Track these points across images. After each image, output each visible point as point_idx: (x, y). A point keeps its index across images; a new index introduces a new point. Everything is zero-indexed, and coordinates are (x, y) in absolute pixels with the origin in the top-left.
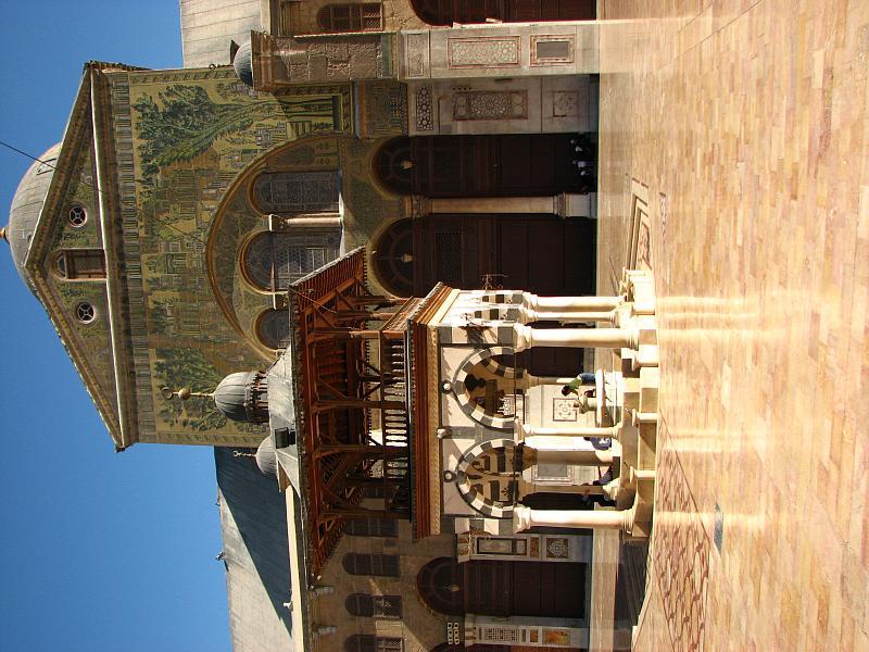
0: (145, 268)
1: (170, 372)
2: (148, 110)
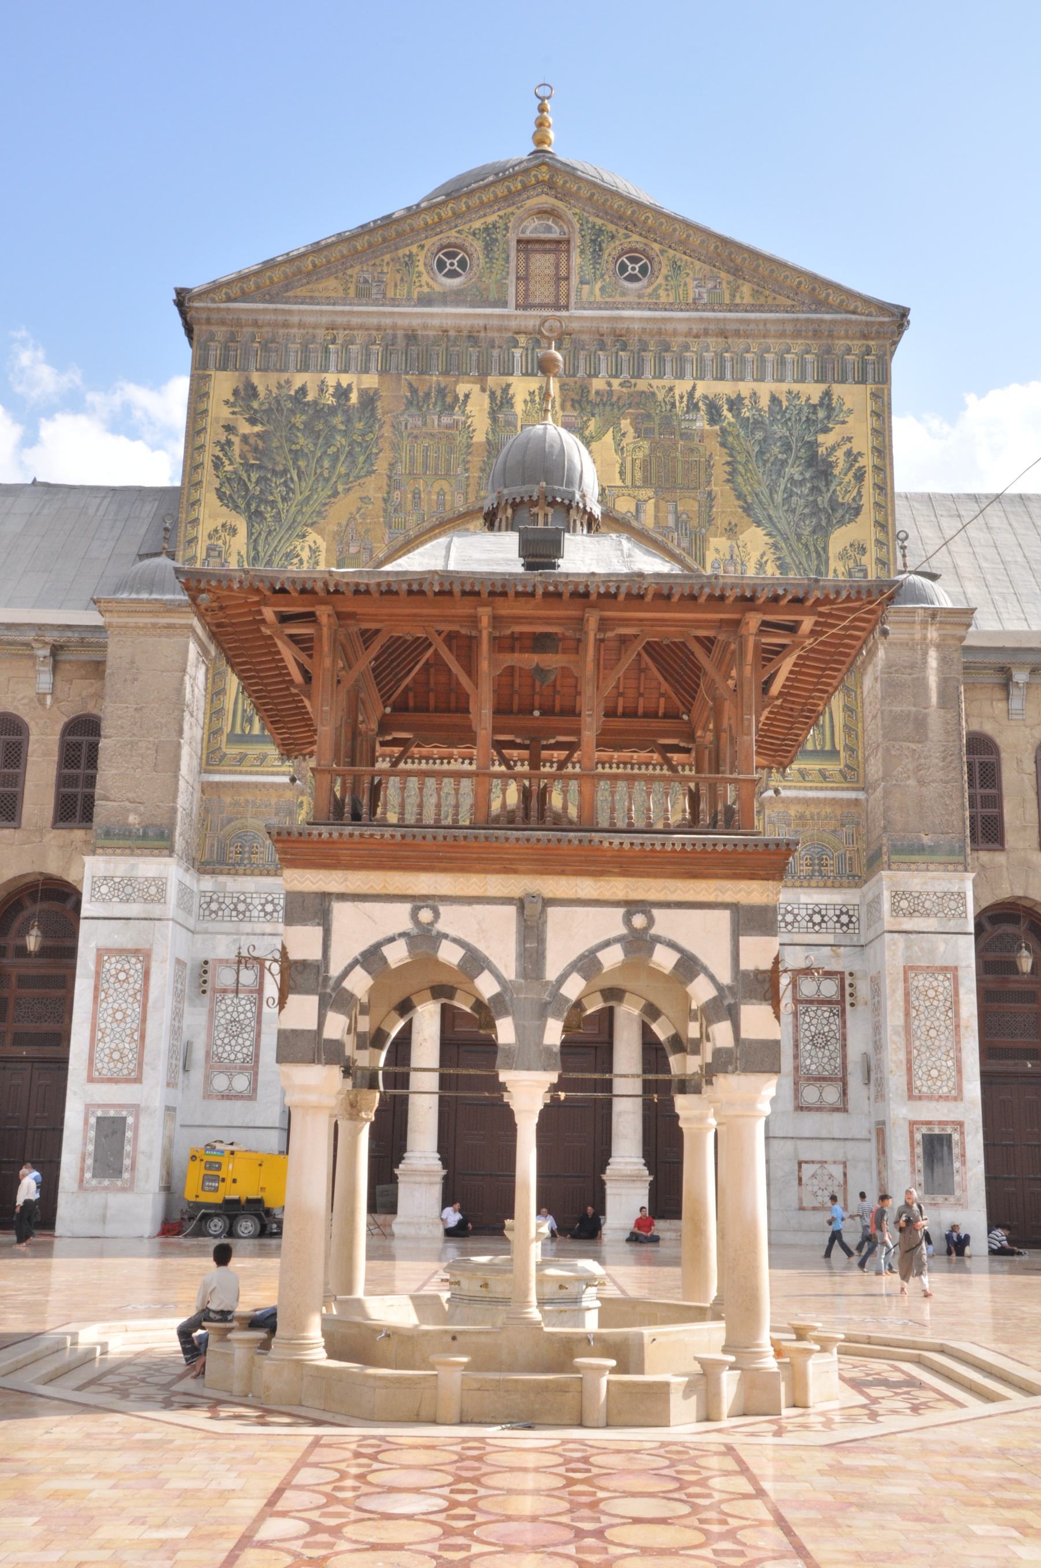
0: (534, 384)
1: (333, 410)
2: (821, 414)
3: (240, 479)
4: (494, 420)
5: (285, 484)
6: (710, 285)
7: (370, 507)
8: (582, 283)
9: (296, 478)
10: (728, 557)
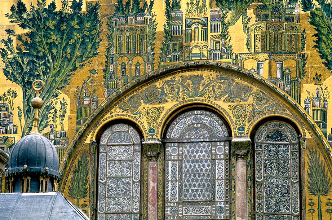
1: (71, 17)
3: (18, 62)
4: (169, 17)
5: (45, 64)
7: (96, 75)
9: (51, 60)
10: (315, 96)
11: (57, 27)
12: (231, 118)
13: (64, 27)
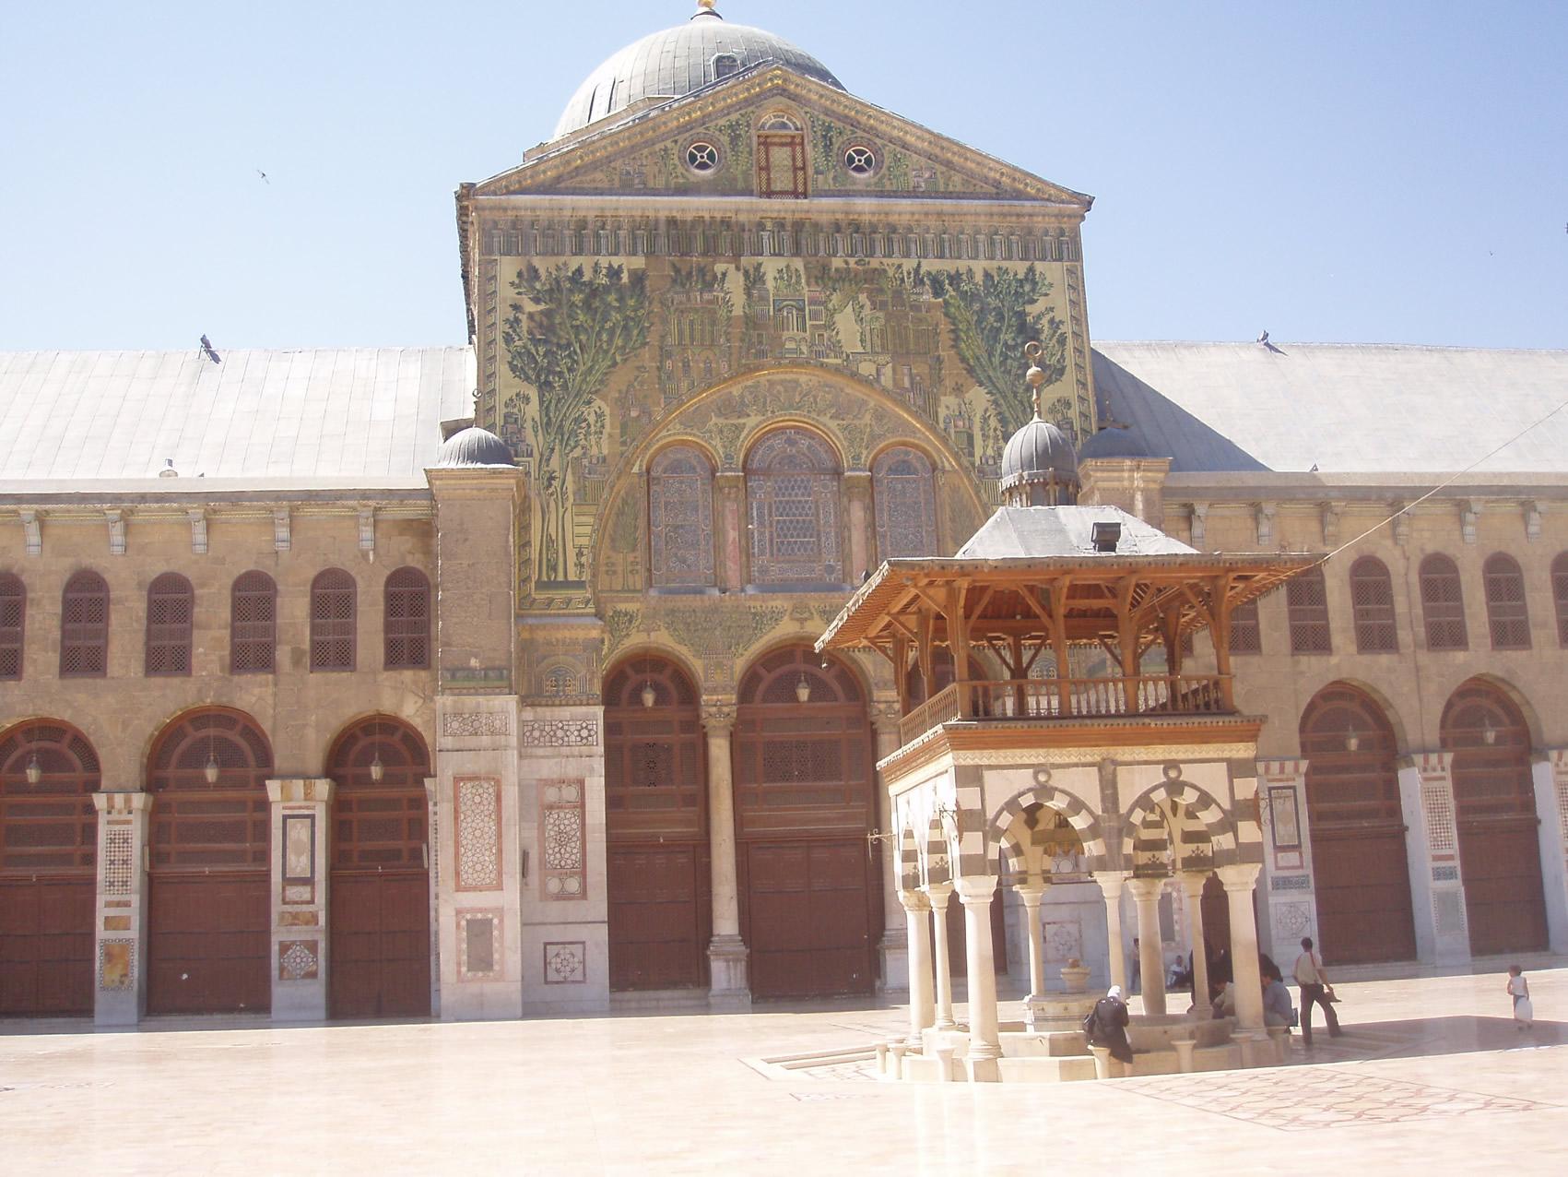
0: (781, 263)
1: (607, 289)
2: (1027, 288)
3: (529, 352)
4: (749, 295)
5: (569, 356)
6: (927, 175)
8: (818, 172)
11: (587, 305)
12: (840, 443)
13: (597, 303)
